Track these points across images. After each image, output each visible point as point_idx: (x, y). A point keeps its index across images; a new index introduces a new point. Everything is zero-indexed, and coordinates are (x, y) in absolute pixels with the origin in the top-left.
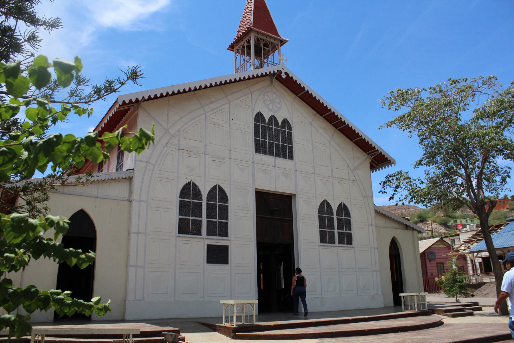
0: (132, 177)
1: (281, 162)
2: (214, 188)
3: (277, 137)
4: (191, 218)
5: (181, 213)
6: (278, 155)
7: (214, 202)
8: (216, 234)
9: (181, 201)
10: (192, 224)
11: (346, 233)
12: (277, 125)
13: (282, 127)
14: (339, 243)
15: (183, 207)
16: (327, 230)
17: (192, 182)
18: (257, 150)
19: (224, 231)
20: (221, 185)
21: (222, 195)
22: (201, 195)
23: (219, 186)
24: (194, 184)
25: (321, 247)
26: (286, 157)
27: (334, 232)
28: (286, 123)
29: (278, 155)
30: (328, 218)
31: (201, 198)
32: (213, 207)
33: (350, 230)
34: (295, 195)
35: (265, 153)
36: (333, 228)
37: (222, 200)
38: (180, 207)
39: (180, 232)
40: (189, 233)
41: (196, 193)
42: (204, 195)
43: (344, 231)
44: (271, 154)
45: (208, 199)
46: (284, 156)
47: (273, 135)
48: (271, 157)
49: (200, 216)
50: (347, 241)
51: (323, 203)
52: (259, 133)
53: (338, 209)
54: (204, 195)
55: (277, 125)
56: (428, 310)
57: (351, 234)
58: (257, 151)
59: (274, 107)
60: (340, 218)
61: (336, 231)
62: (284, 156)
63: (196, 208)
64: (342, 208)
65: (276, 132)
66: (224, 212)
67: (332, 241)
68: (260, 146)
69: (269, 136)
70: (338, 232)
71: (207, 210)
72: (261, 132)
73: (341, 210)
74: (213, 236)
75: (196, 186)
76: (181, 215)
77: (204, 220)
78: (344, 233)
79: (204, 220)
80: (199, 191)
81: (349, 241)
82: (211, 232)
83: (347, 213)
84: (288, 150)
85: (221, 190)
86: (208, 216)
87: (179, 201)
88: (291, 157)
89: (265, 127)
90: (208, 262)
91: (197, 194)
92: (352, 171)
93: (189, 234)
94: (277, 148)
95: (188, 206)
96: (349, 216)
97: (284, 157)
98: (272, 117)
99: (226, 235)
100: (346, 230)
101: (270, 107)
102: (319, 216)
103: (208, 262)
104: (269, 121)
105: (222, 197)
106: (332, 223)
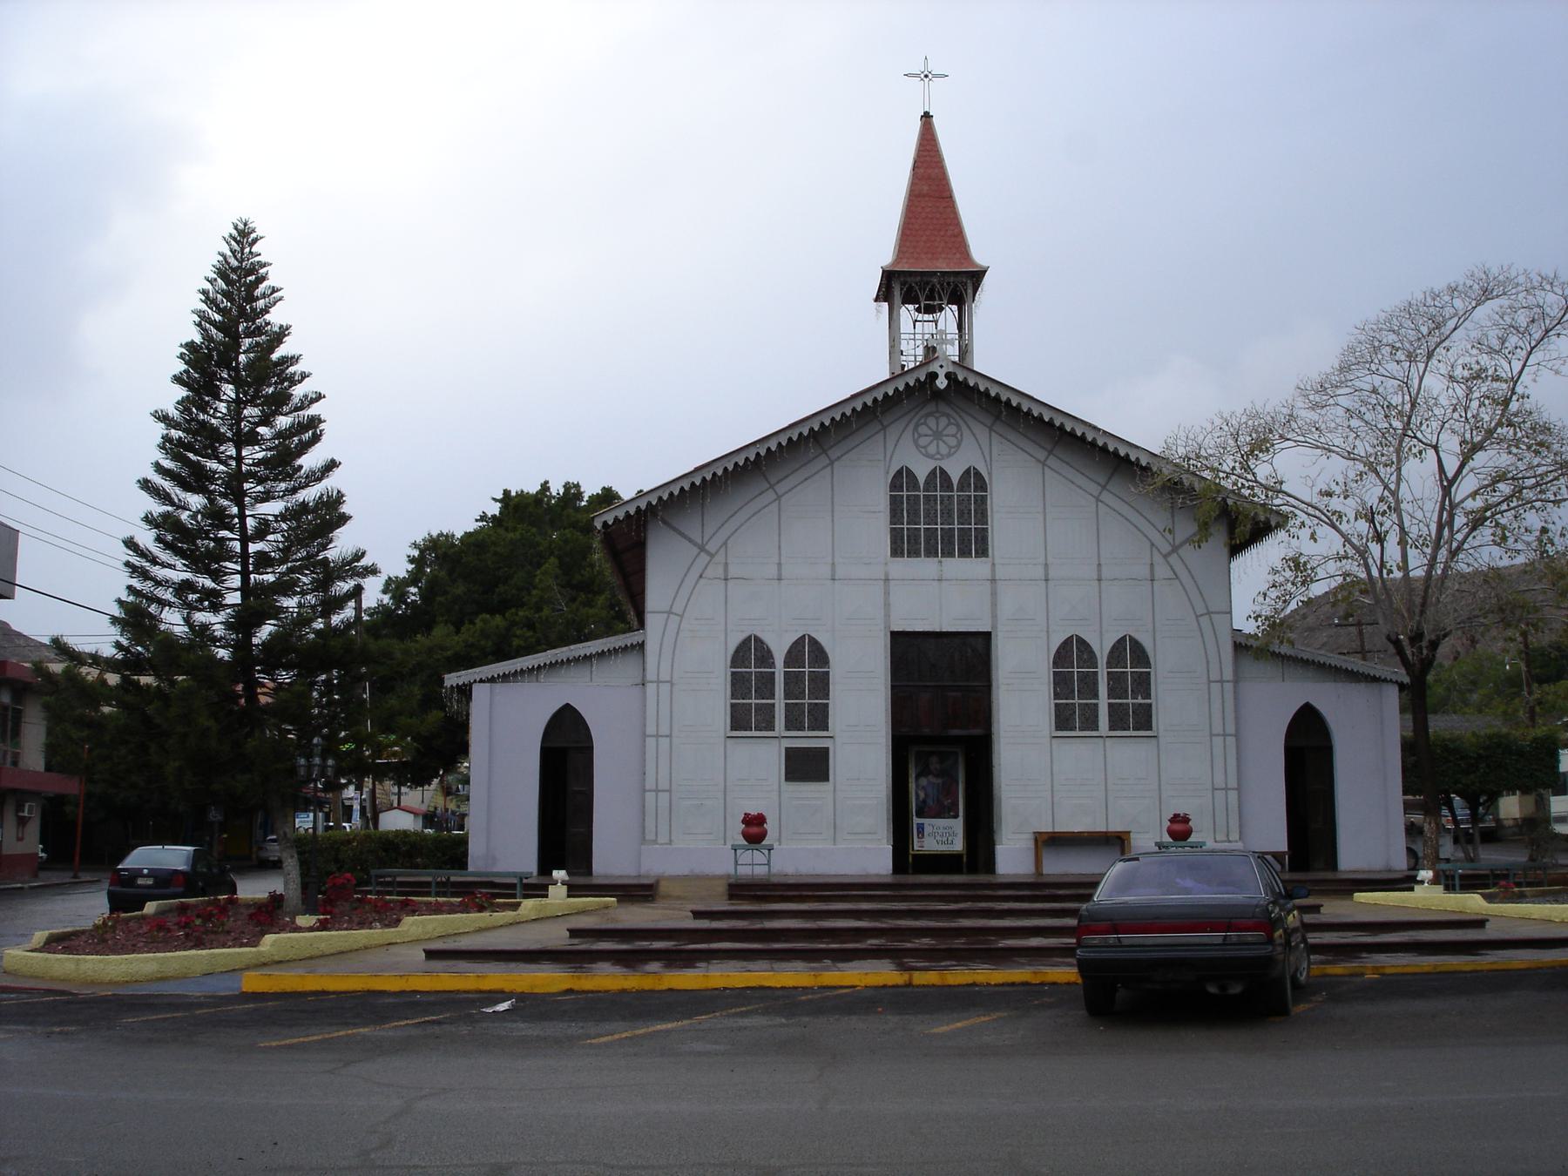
0: (643, 642)
1: (956, 566)
3: (947, 514)
9: (733, 674)
16: (1076, 701)
17: (755, 636)
18: (896, 551)
19: (820, 719)
24: (758, 640)
25: (1054, 741)
31: (773, 663)
33: (1148, 696)
35: (913, 552)
38: (733, 684)
43: (1130, 701)
44: (932, 552)
49: (772, 696)
50: (1135, 723)
51: (1067, 643)
60: (1117, 672)
62: (964, 553)
65: (946, 502)
66: (822, 684)
67: (1090, 722)
69: (927, 515)
71: (786, 684)
72: (907, 511)
74: (799, 730)
79: (780, 702)
80: (769, 651)
81: (1143, 720)
82: (793, 723)
85: (814, 643)
88: (983, 552)
90: (787, 779)
91: (765, 656)
92: (1165, 556)
94: (946, 539)
96: (1148, 665)
97: (965, 553)
98: (936, 471)
99: (826, 728)
101: (932, 449)
103: (787, 779)
104: (927, 483)
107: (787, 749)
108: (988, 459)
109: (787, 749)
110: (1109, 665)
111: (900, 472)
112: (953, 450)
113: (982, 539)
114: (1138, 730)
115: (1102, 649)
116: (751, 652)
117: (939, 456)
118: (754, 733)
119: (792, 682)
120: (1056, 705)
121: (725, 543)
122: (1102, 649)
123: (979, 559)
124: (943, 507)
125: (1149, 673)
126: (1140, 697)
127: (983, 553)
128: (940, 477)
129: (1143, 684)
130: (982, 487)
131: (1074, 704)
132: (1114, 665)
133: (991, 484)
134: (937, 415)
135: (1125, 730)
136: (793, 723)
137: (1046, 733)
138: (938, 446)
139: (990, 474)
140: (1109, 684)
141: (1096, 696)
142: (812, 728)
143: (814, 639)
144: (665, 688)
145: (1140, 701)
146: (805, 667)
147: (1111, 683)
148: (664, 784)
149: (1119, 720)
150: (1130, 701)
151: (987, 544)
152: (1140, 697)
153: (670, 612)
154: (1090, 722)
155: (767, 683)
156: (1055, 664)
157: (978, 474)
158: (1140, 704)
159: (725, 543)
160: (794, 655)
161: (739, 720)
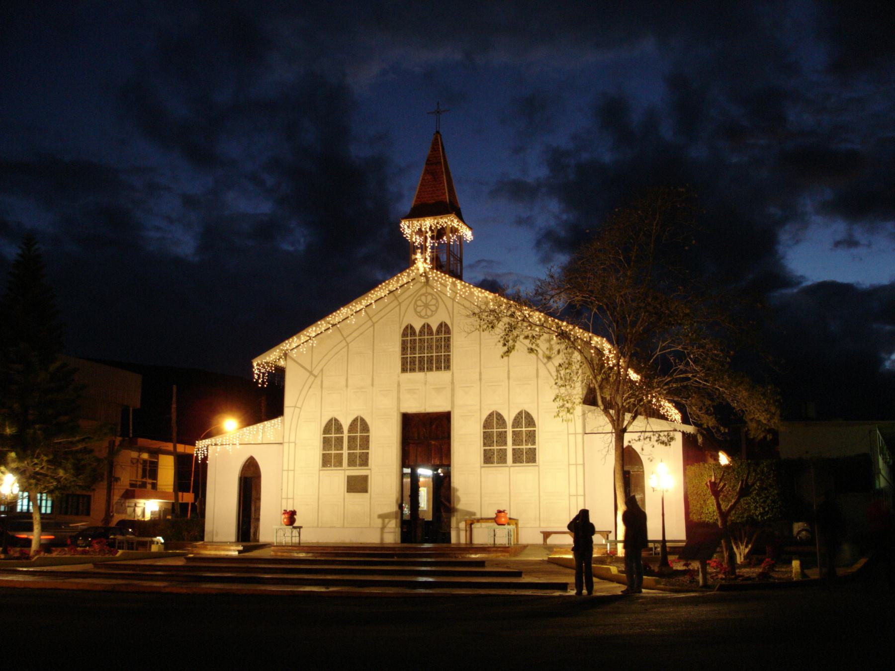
2: (355, 421)
5: (324, 449)
6: (430, 369)
11: (526, 449)
18: (404, 370)
19: (364, 461)
20: (364, 417)
24: (336, 420)
30: (498, 432)
31: (343, 431)
35: (413, 370)
38: (324, 443)
42: (346, 428)
43: (524, 447)
44: (421, 369)
54: (346, 428)
55: (431, 333)
57: (535, 449)
59: (424, 311)
62: (438, 368)
64: (522, 418)
66: (365, 443)
67: (502, 459)
70: (514, 449)
73: (521, 420)
75: (338, 421)
79: (345, 452)
80: (341, 425)
81: (531, 457)
82: (352, 463)
84: (444, 359)
86: (349, 448)
88: (448, 368)
89: (415, 340)
90: (348, 492)
91: (339, 428)
96: (534, 425)
97: (438, 368)
100: (526, 445)
103: (348, 492)
104: (420, 332)
106: (503, 439)
107: (348, 477)
108: (451, 316)
109: (348, 477)
110: (513, 426)
111: (407, 327)
112: (434, 313)
113: (448, 361)
115: (509, 418)
116: (333, 426)
117: (426, 317)
118: (333, 468)
119: (352, 440)
121: (322, 370)
122: (509, 418)
123: (446, 372)
125: (535, 431)
126: (530, 444)
127: (448, 368)
128: (427, 328)
129: (532, 437)
131: (494, 450)
133: (453, 331)
134: (427, 294)
135: (521, 463)
136: (352, 463)
137: (478, 465)
138: (426, 311)
139: (452, 325)
140: (513, 437)
141: (506, 444)
144: (292, 445)
145: (530, 446)
147: (514, 436)
148: (290, 496)
149: (518, 458)
150: (524, 447)
151: (450, 363)
152: (530, 444)
153: (295, 407)
154: (502, 459)
155: (340, 441)
156: (485, 427)
157: (446, 325)
158: (530, 448)
159: (322, 370)
160: (353, 427)
161: (326, 461)
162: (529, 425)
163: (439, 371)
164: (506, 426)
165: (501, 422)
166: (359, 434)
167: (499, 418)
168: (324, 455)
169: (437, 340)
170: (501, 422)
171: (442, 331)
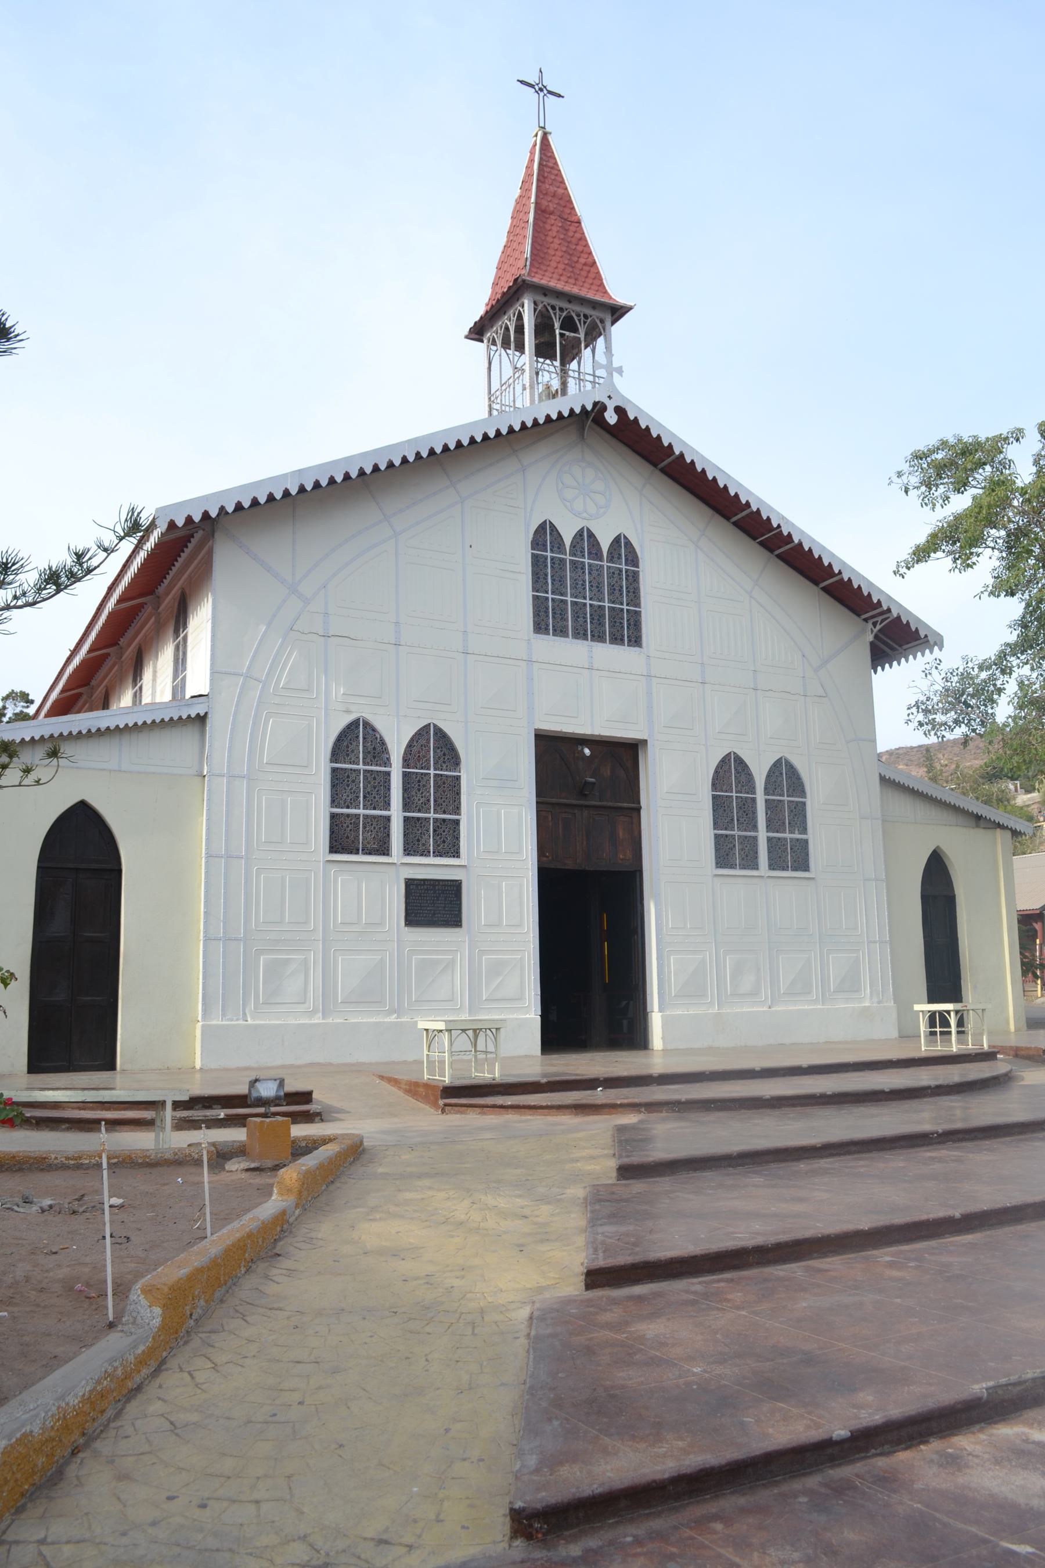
0: (206, 713)
1: (607, 653)
3: (597, 587)
4: (361, 811)
6: (599, 637)
7: (422, 768)
8: (429, 852)
9: (334, 771)
10: (364, 827)
11: (792, 840)
12: (596, 554)
13: (611, 559)
14: (772, 867)
15: (341, 783)
19: (448, 842)
21: (444, 749)
22: (388, 753)
23: (435, 726)
24: (366, 724)
25: (716, 879)
26: (622, 640)
27: (755, 839)
28: (623, 549)
29: (599, 637)
31: (388, 759)
32: (419, 781)
33: (804, 831)
34: (645, 742)
35: (560, 631)
36: (755, 828)
37: (444, 762)
39: (333, 849)
40: (358, 850)
41: (374, 749)
43: (787, 835)
44: (580, 634)
45: (406, 762)
46: (616, 639)
47: (584, 581)
48: (579, 641)
49: (387, 805)
51: (725, 761)
52: (546, 578)
53: (768, 776)
55: (596, 554)
56: (989, 1047)
57: (806, 841)
58: (540, 628)
60: (774, 800)
61: (762, 835)
63: (375, 788)
67: (750, 861)
68: (548, 616)
69: (574, 586)
70: (769, 839)
71: (405, 789)
73: (780, 779)
75: (374, 730)
76: (336, 807)
77: (396, 813)
78: (785, 839)
79: (396, 813)
80: (383, 743)
83: (797, 785)
84: (628, 621)
85: (442, 737)
86: (407, 806)
87: (329, 771)
88: (636, 641)
89: (562, 561)
91: (378, 750)
93: (357, 853)
95: (353, 781)
96: (802, 793)
97: (617, 639)
98: (583, 532)
99: (456, 854)
100: (791, 832)
102: (714, 797)
104: (573, 546)
105: (444, 754)
106: (750, 815)
107: (410, 883)
109: (410, 883)
111: (542, 527)
113: (635, 625)
114: (797, 870)
117: (585, 515)
120: (716, 835)
124: (592, 578)
125: (804, 804)
126: (797, 832)
127: (636, 642)
128: (586, 539)
129: (799, 816)
130: (633, 561)
131: (733, 836)
132: (771, 792)
140: (767, 814)
142: (439, 854)
143: (440, 730)
145: (797, 836)
146: (429, 769)
147: (769, 813)
152: (797, 832)
156: (714, 786)
160: (414, 752)
162: (794, 790)
163: (617, 644)
164: (754, 788)
165: (743, 778)
166: (432, 772)
167: (740, 770)
168: (333, 817)
169: (611, 575)
170: (743, 778)
171: (620, 555)
